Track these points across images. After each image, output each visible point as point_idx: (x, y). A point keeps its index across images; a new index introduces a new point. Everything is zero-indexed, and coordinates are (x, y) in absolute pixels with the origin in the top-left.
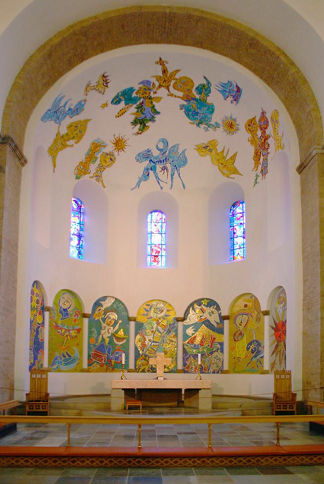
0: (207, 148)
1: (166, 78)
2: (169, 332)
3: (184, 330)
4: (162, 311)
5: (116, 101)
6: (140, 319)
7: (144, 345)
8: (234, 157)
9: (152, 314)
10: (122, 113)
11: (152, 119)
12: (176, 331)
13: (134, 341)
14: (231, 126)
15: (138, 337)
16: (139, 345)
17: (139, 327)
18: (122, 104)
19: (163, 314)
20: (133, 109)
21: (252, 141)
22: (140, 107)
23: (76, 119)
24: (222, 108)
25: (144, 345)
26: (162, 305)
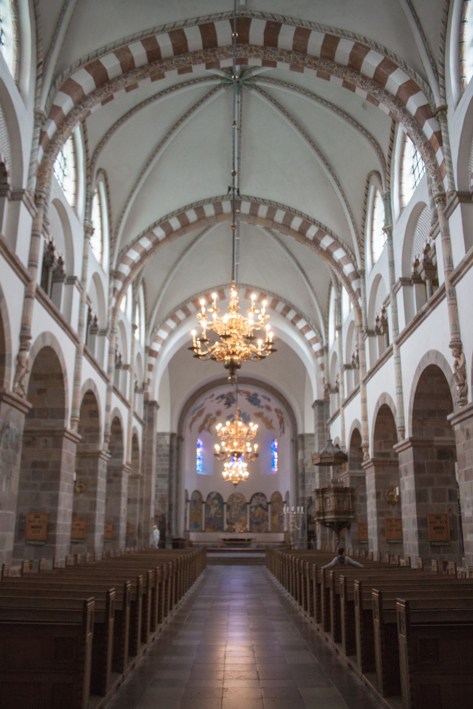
0: (259, 415)
1: (238, 391)
2: (243, 510)
3: (250, 509)
4: (239, 499)
5: (217, 398)
6: (230, 503)
7: (231, 518)
8: (271, 421)
9: (235, 500)
10: (220, 402)
11: (233, 402)
12: (246, 510)
13: (226, 515)
14: (268, 408)
15: (228, 513)
16: (229, 517)
17: (229, 508)
18: (220, 399)
19: (241, 500)
20: (225, 400)
21: (278, 416)
22: (228, 399)
23: (200, 409)
24: (264, 402)
25: (231, 518)
26: (239, 496)
